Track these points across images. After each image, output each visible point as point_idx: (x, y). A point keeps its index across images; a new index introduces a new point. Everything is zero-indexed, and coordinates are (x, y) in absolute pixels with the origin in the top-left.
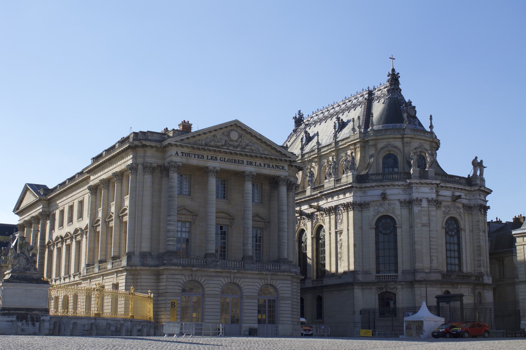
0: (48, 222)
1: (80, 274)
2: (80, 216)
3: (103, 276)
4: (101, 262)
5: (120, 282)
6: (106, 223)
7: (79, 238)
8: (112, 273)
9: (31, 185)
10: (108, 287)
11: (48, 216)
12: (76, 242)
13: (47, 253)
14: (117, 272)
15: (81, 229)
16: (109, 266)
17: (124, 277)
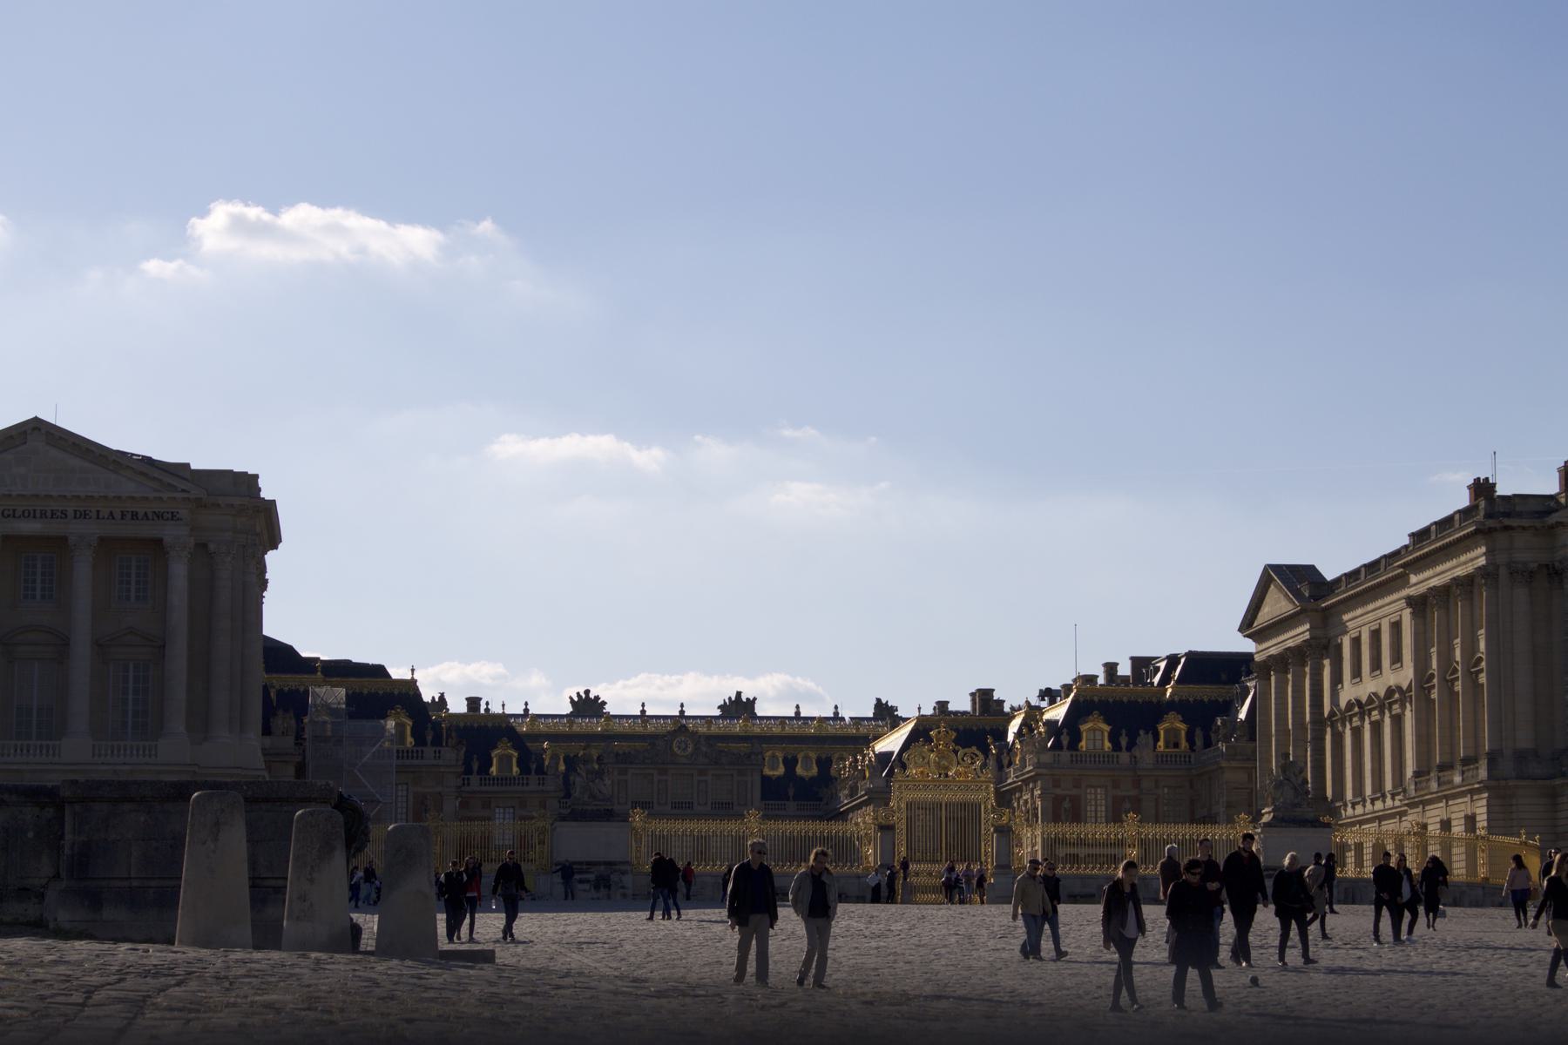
0: (1327, 662)
1: (1405, 791)
2: (1397, 658)
3: (1447, 798)
4: (1445, 767)
5: (1478, 811)
6: (1448, 684)
7: (1396, 708)
8: (1462, 794)
9: (1277, 569)
10: (1434, 829)
11: (1326, 647)
12: (1392, 717)
13: (1328, 737)
14: (1472, 792)
15: (1399, 688)
16: (1457, 779)
17: (1484, 802)
